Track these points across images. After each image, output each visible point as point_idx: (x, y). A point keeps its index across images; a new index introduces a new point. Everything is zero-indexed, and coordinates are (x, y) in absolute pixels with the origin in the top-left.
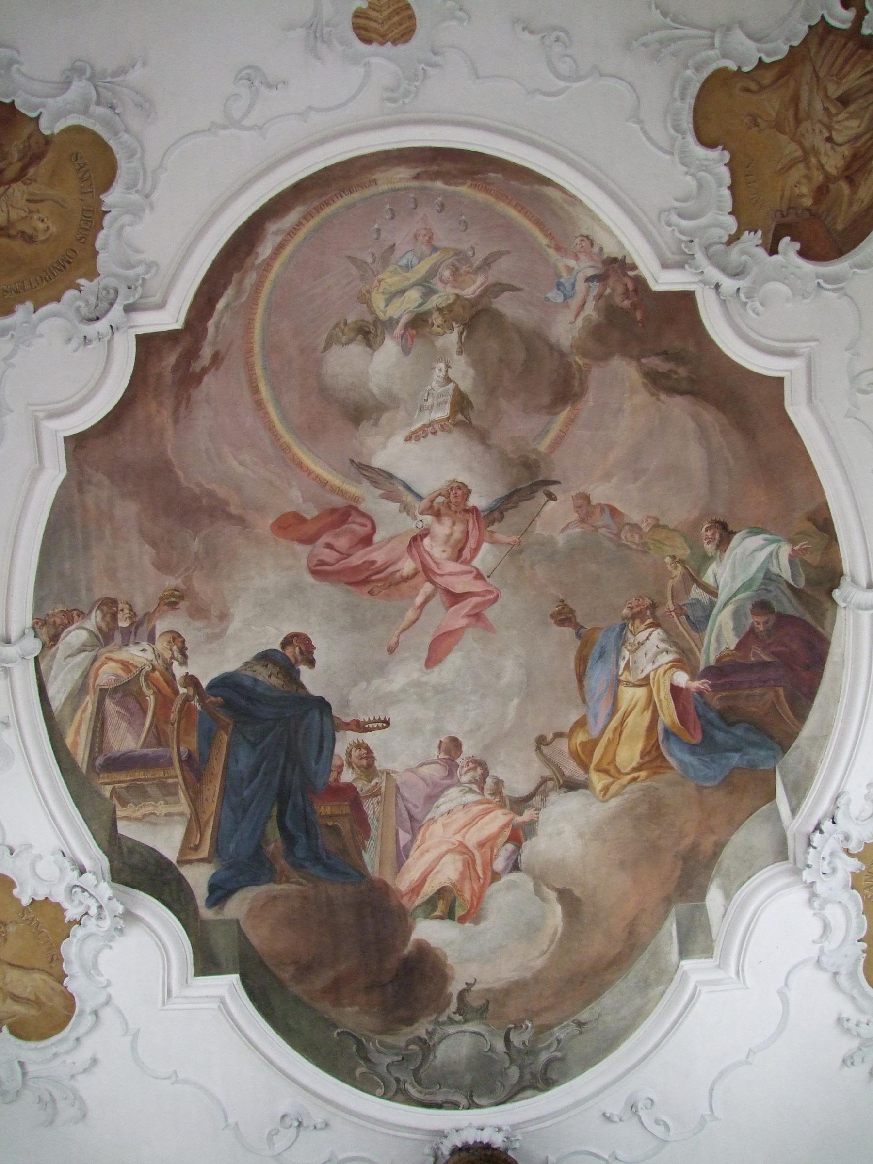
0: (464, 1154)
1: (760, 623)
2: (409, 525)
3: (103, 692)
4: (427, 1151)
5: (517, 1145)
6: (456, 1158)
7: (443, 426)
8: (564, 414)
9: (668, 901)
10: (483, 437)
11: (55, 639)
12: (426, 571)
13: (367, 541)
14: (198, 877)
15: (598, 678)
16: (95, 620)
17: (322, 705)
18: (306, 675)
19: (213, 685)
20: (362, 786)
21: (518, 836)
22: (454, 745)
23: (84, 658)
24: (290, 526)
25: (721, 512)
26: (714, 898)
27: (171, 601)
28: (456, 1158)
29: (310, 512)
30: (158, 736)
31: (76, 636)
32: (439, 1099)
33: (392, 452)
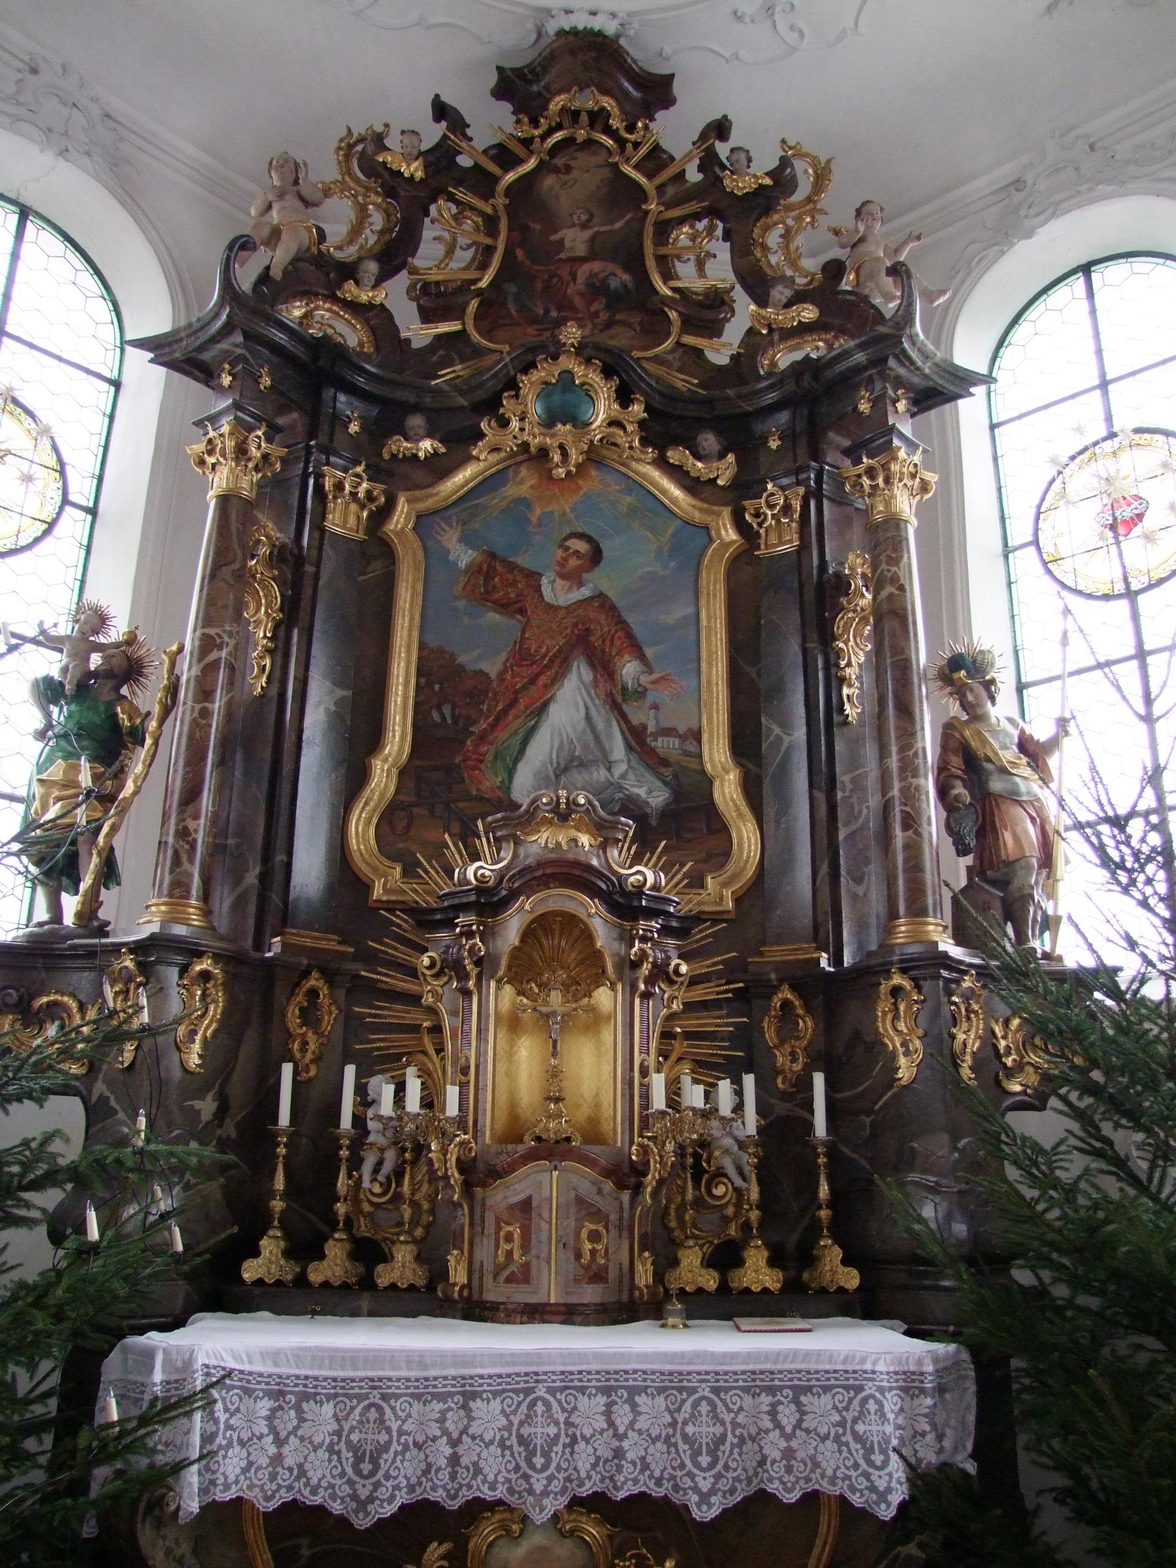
0: (571, 38)
4: (530, 26)
5: (632, 33)
6: (562, 41)
28: (562, 41)
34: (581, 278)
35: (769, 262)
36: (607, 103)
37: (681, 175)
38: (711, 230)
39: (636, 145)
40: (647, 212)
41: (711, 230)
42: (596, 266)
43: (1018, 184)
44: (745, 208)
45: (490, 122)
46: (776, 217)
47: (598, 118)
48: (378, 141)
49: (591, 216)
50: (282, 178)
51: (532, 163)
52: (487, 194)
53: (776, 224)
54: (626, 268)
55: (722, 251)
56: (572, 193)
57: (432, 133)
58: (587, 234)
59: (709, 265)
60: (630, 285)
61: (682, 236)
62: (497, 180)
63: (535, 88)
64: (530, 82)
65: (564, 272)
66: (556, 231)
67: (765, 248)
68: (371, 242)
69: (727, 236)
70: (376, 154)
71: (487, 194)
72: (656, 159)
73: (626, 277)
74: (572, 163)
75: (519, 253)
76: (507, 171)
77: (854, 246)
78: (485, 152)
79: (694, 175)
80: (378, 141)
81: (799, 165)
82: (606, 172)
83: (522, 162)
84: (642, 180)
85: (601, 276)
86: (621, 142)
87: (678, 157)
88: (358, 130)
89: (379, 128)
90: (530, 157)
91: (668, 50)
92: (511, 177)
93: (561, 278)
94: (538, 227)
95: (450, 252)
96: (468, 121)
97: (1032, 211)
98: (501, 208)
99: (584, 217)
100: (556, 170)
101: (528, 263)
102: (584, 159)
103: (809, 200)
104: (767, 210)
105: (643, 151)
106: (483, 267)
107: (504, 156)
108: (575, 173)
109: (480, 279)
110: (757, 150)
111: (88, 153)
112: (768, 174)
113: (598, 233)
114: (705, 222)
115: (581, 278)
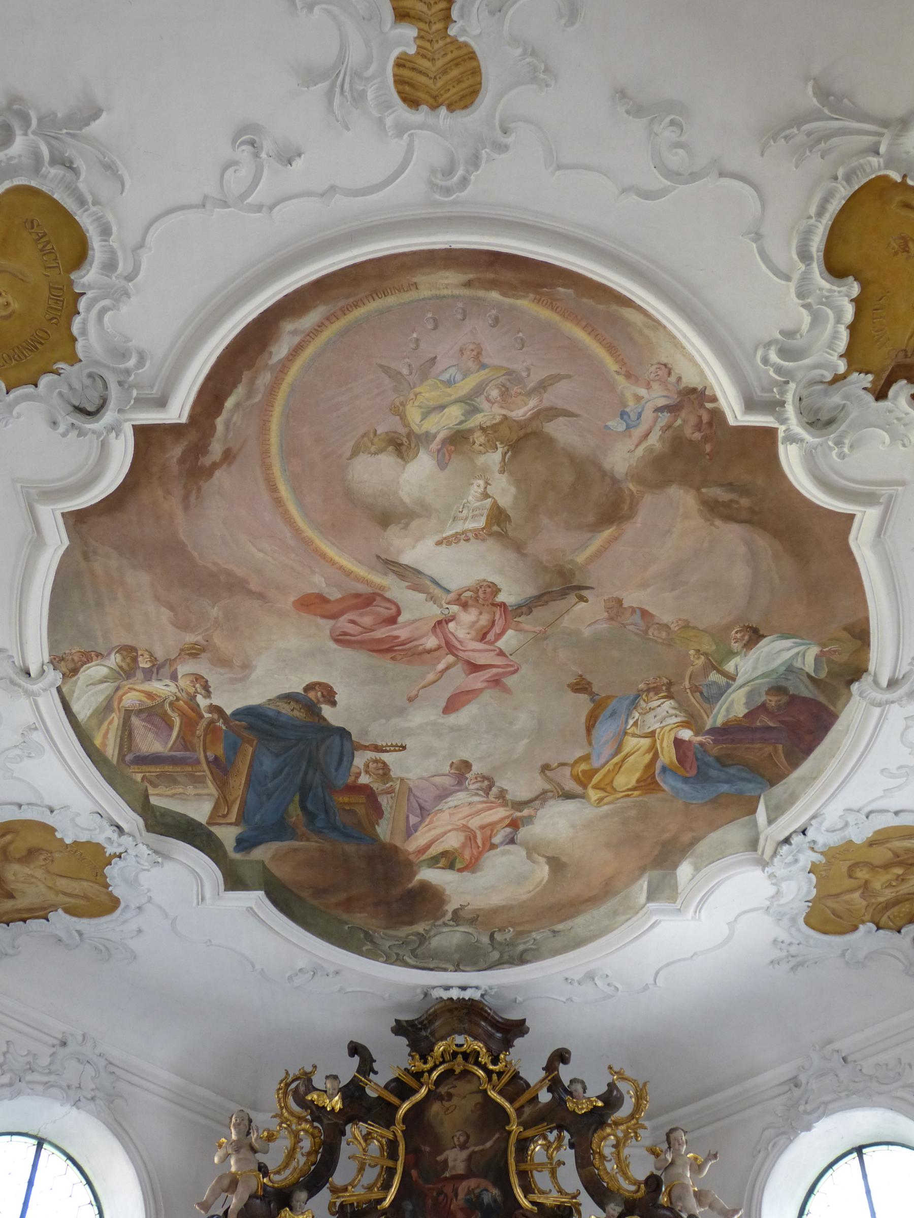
1: (773, 701)
2: (434, 612)
3: (128, 713)
7: (477, 534)
8: (607, 533)
9: (643, 870)
10: (518, 547)
11: (75, 671)
12: (450, 648)
13: (392, 621)
14: (227, 835)
15: (605, 731)
16: (114, 660)
17: (343, 733)
18: (327, 711)
19: (237, 714)
20: (377, 786)
21: (515, 824)
22: (466, 765)
23: (106, 688)
24: (313, 604)
25: (754, 621)
26: (685, 870)
27: (194, 652)
29: (334, 594)
30: (185, 742)
31: (95, 670)
32: (432, 966)
33: (419, 551)
34: (461, 1196)
35: (605, 1169)
36: (478, 1046)
37: (535, 1098)
38: (560, 1138)
39: (500, 1074)
40: (510, 1133)
41: (560, 1138)
42: (473, 1183)
43: (795, 1082)
44: (585, 1125)
45: (393, 1059)
46: (608, 1130)
47: (471, 1056)
48: (306, 1078)
49: (468, 1137)
50: (238, 1133)
51: (423, 1091)
52: (389, 1123)
53: (609, 1135)
54: (495, 1184)
55: (568, 1155)
56: (452, 1118)
57: (348, 1069)
58: (464, 1154)
59: (560, 1171)
60: (499, 1199)
61: (537, 1149)
62: (397, 1108)
63: (424, 1033)
64: (421, 1029)
65: (448, 1190)
66: (441, 1153)
67: (603, 1157)
68: (301, 1163)
69: (572, 1146)
70: (307, 1094)
71: (389, 1123)
72: (515, 1086)
73: (495, 1192)
74: (452, 1091)
75: (414, 1173)
76: (403, 1099)
77: (666, 1168)
78: (386, 1087)
79: (545, 1097)
80: (306, 1078)
81: (623, 1086)
82: (478, 1098)
83: (415, 1092)
84: (507, 1105)
85: (477, 1191)
86: (489, 1073)
87: (532, 1083)
88: (294, 1072)
89: (309, 1069)
90: (421, 1088)
91: (520, 999)
92: (405, 1106)
93: (446, 1195)
94: (428, 1149)
95: (361, 1169)
96: (374, 1058)
97: (809, 1107)
98: (399, 1134)
99: (462, 1139)
100: (441, 1098)
101: (421, 1181)
102: (462, 1087)
103: (632, 1117)
104: (602, 1124)
105: (505, 1079)
106: (387, 1186)
107: (401, 1089)
108: (455, 1100)
109: (384, 1199)
110: (589, 1078)
111: (93, 1099)
112: (599, 1097)
113: (473, 1152)
114: (555, 1132)
115: (461, 1196)
